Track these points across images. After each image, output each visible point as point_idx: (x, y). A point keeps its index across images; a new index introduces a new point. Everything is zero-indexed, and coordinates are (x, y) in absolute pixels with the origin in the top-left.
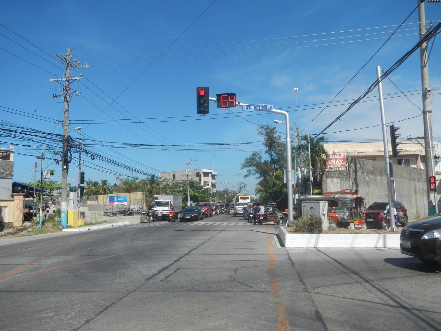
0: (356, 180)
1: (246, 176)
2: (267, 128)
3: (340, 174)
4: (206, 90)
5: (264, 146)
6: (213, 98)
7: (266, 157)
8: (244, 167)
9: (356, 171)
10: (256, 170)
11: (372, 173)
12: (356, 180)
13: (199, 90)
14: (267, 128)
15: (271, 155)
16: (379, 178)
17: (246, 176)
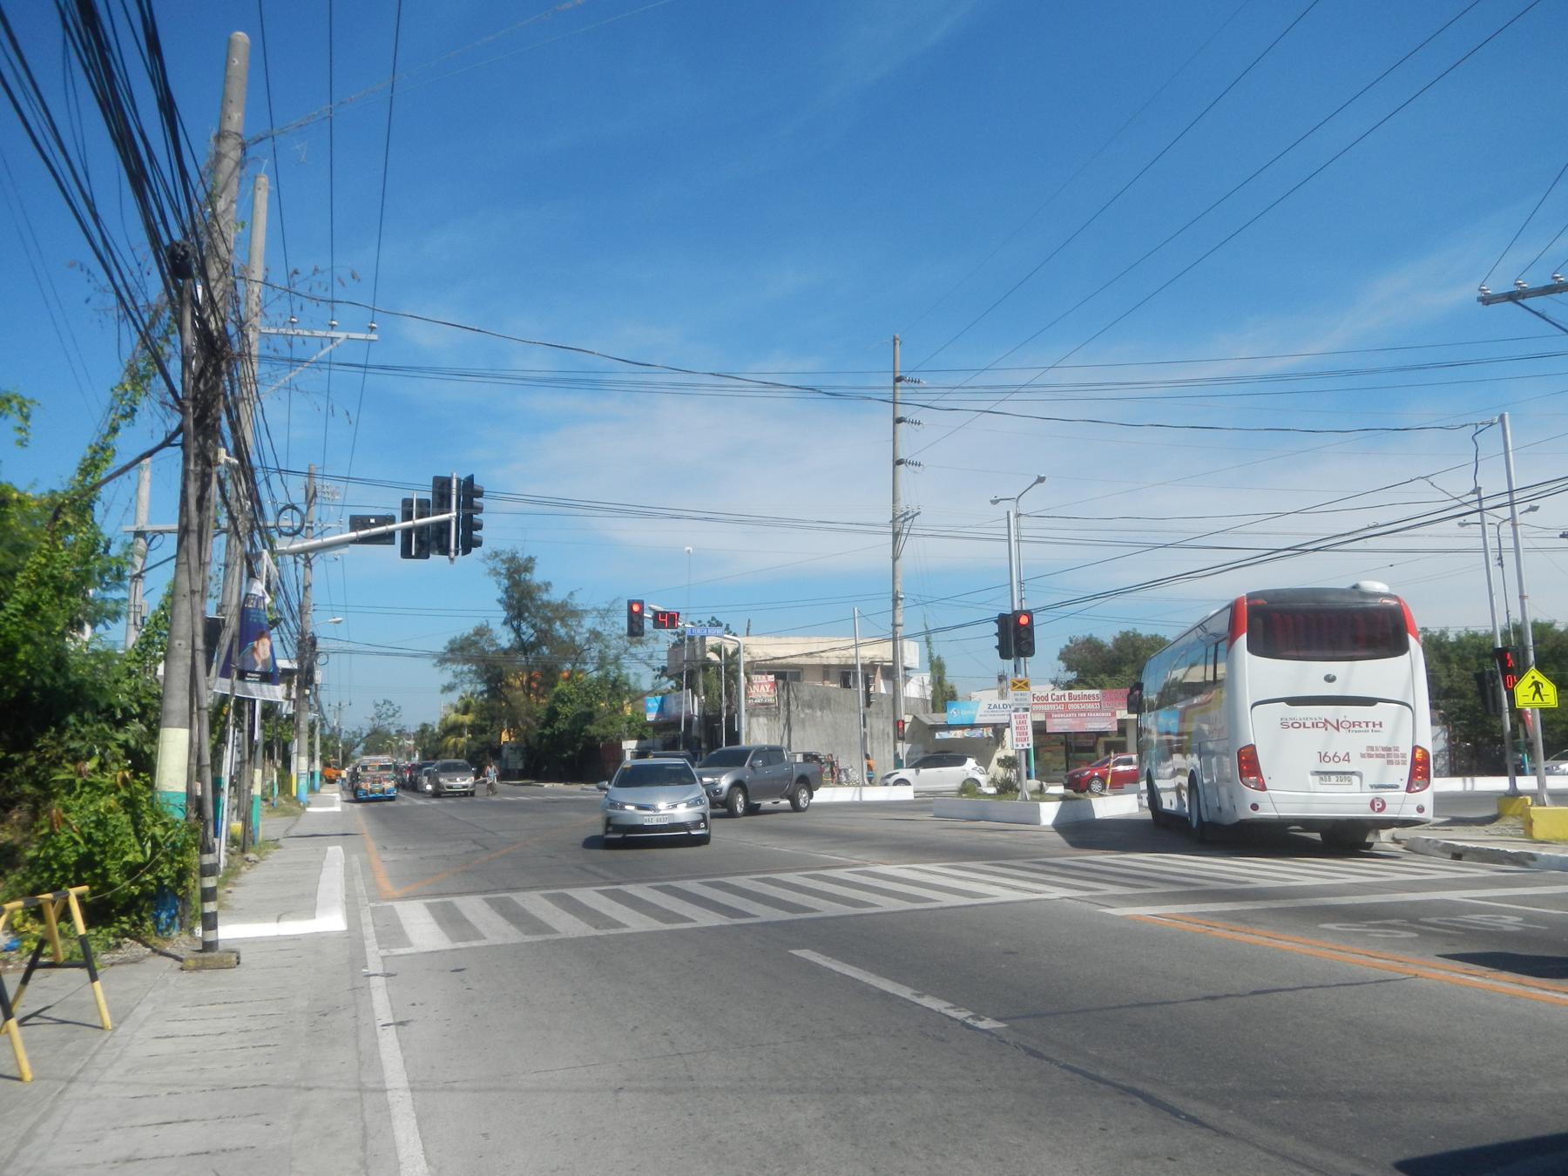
0: (788, 719)
1: (449, 688)
2: (513, 559)
3: (764, 708)
4: (641, 603)
5: (500, 607)
6: (648, 615)
7: (505, 638)
8: (443, 660)
9: (788, 704)
10: (476, 672)
11: (810, 706)
12: (788, 719)
13: (631, 604)
14: (513, 559)
15: (518, 631)
16: (819, 713)
17: (449, 688)
